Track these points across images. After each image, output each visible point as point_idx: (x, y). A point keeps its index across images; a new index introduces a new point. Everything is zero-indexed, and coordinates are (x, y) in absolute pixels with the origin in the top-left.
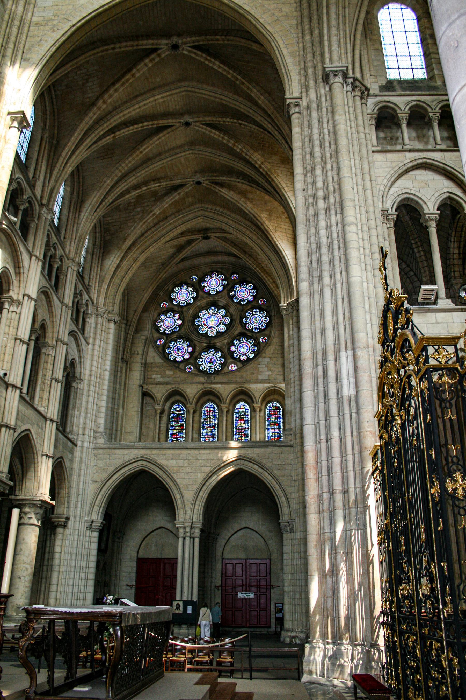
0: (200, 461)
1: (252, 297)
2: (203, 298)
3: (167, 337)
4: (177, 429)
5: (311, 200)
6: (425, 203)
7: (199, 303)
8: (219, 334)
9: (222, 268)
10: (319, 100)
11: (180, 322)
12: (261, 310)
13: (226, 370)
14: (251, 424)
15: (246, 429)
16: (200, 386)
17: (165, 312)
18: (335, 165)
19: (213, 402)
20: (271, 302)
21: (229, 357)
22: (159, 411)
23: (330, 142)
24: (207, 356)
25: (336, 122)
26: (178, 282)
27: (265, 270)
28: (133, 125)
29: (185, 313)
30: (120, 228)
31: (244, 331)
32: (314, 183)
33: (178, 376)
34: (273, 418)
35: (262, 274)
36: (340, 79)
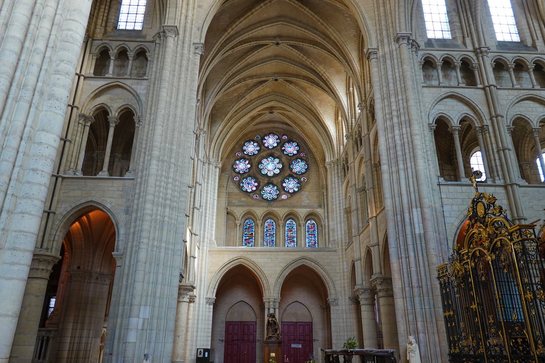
0: (279, 259)
1: (296, 151)
2: (264, 151)
3: (241, 176)
4: (249, 236)
5: (388, 116)
6: (452, 120)
7: (262, 154)
8: (275, 175)
9: (276, 132)
10: (391, 52)
11: (249, 166)
12: (302, 160)
13: (280, 199)
14: (297, 234)
15: (293, 237)
16: (266, 209)
17: (239, 159)
18: (404, 97)
19: (272, 219)
20: (309, 155)
21: (282, 190)
22: (238, 225)
23: (400, 81)
24: (268, 189)
25: (404, 70)
26: (248, 139)
27: (308, 135)
28: (245, 43)
29: (252, 160)
30: (222, 106)
31: (291, 173)
32: (390, 105)
33: (249, 201)
34: (311, 230)
35: (306, 138)
36: (405, 41)
